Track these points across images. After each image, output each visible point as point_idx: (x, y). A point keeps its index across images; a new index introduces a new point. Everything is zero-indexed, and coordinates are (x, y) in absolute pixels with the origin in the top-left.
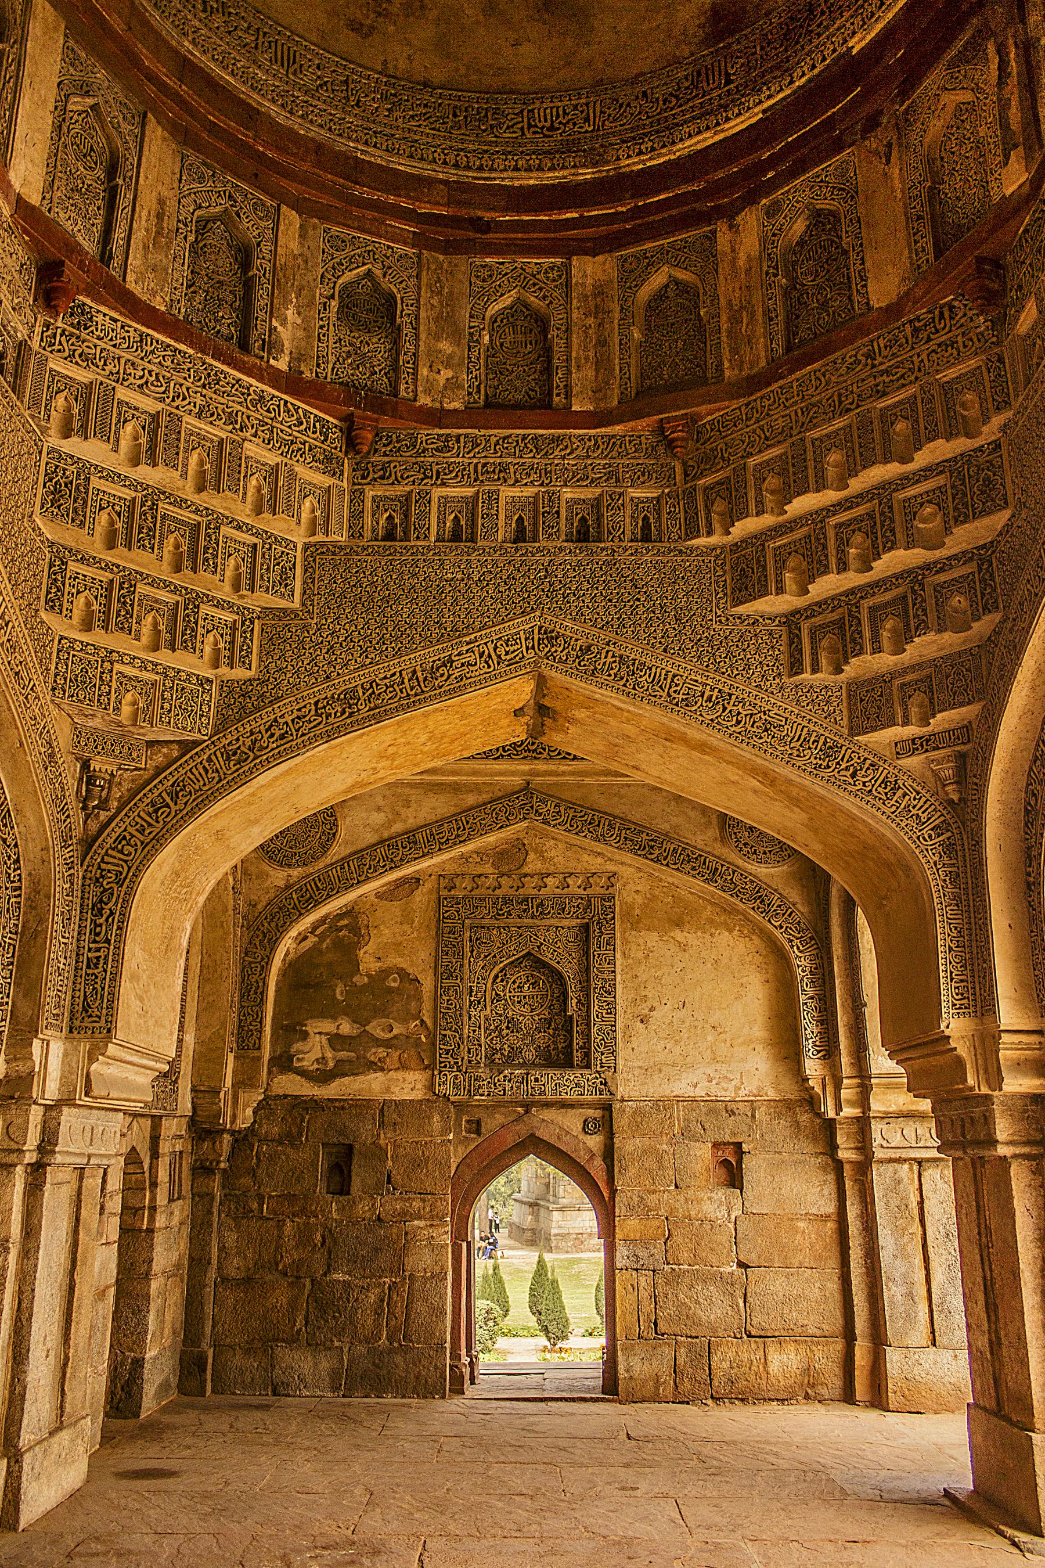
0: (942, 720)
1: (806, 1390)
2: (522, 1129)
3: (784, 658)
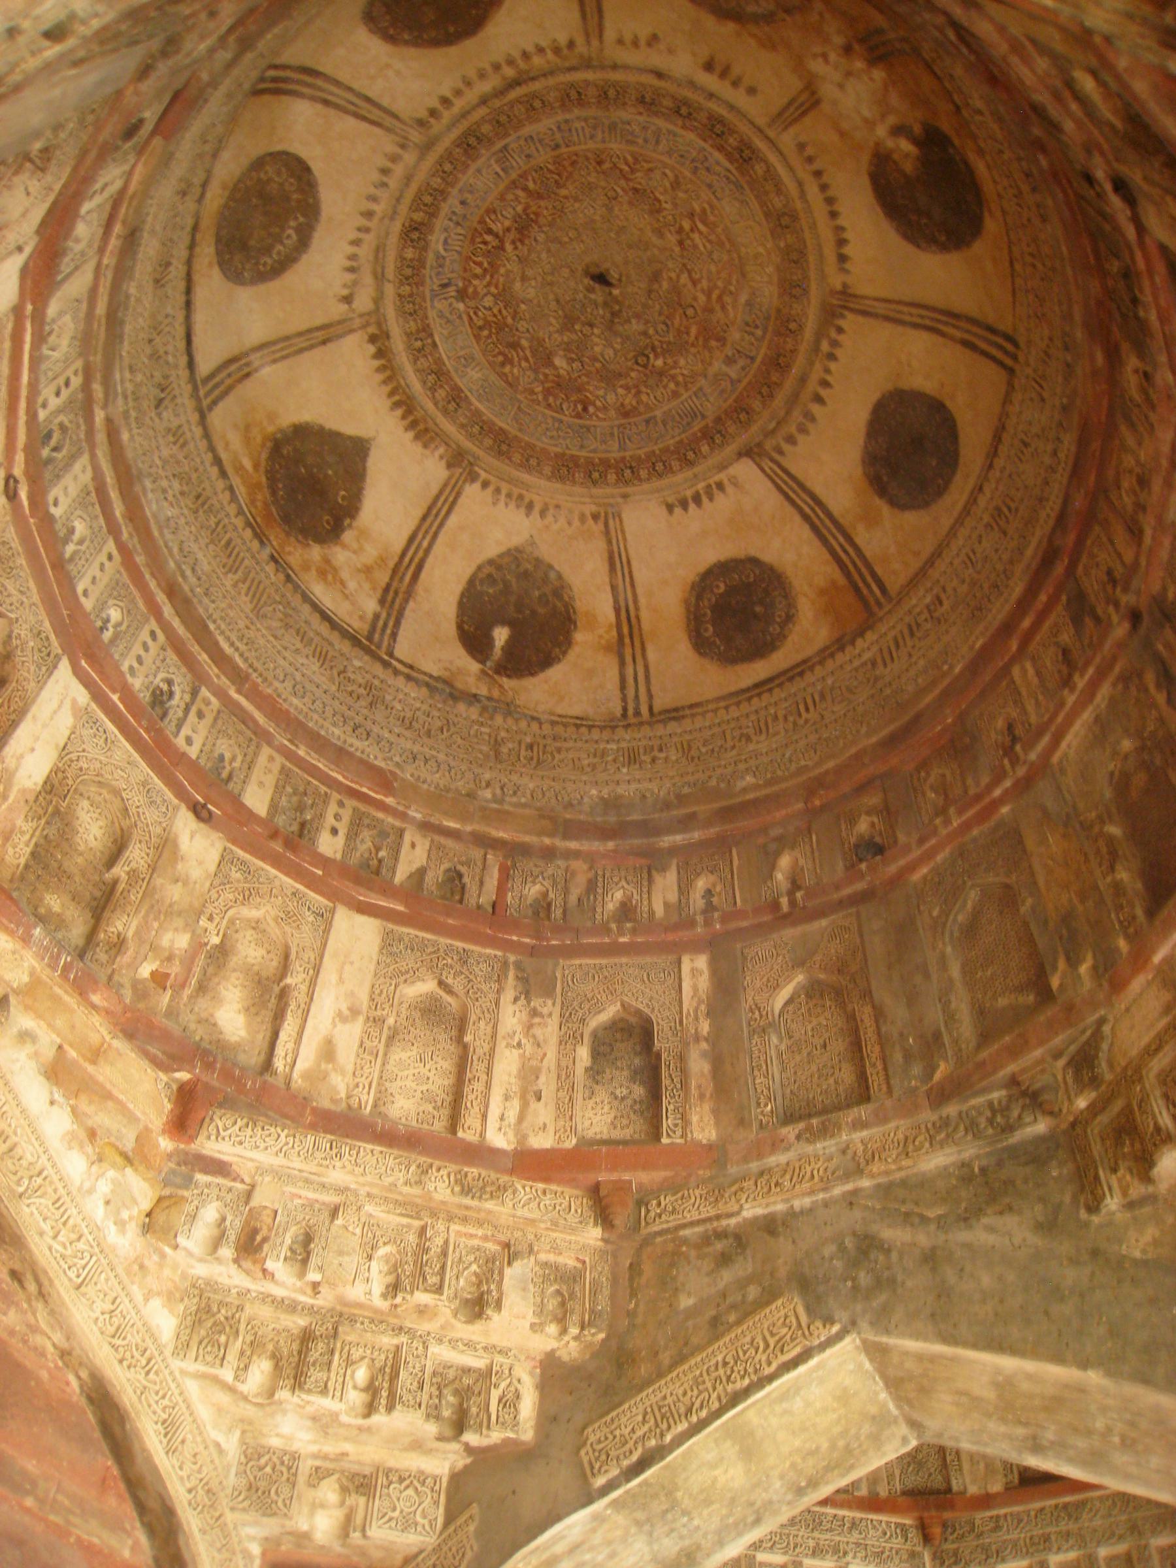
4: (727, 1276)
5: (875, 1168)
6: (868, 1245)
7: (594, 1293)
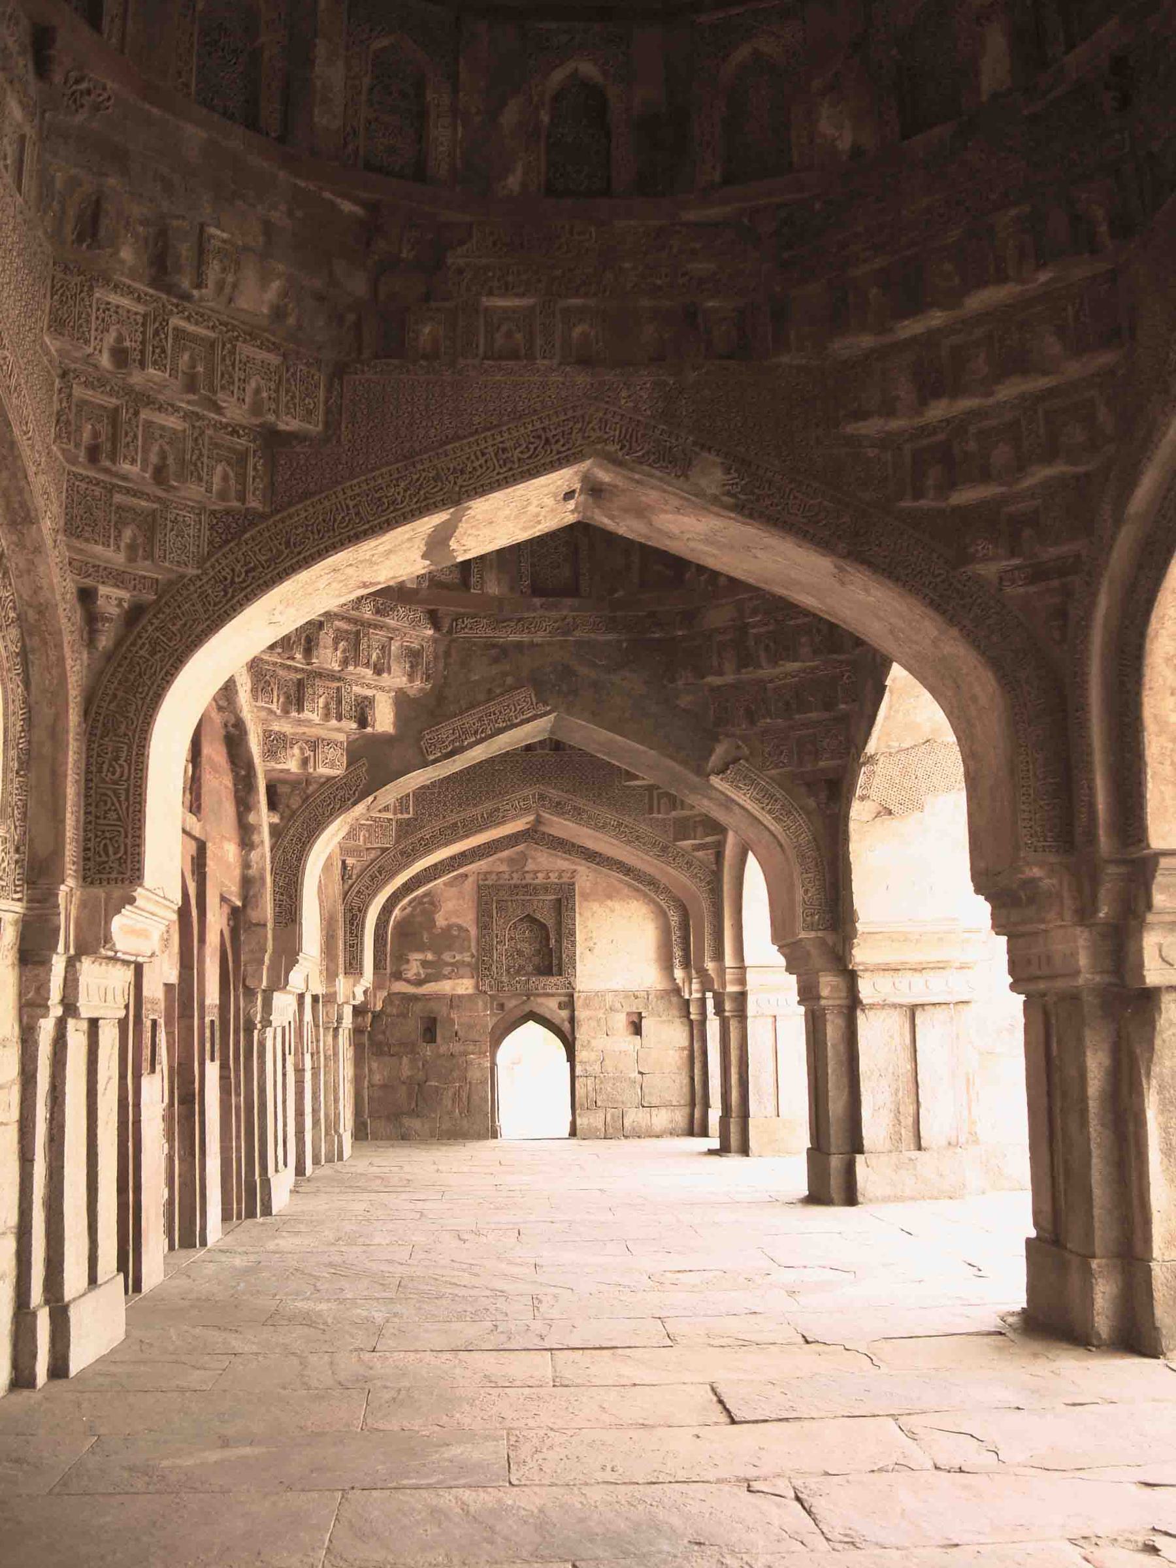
0: (709, 839)
1: (672, 1133)
2: (527, 1009)
3: (647, 807)
4: (494, 670)
5: (577, 633)
6: (567, 672)
7: (428, 664)
